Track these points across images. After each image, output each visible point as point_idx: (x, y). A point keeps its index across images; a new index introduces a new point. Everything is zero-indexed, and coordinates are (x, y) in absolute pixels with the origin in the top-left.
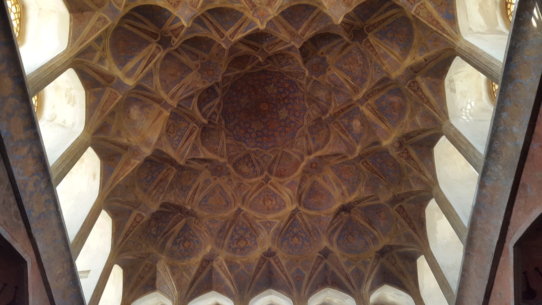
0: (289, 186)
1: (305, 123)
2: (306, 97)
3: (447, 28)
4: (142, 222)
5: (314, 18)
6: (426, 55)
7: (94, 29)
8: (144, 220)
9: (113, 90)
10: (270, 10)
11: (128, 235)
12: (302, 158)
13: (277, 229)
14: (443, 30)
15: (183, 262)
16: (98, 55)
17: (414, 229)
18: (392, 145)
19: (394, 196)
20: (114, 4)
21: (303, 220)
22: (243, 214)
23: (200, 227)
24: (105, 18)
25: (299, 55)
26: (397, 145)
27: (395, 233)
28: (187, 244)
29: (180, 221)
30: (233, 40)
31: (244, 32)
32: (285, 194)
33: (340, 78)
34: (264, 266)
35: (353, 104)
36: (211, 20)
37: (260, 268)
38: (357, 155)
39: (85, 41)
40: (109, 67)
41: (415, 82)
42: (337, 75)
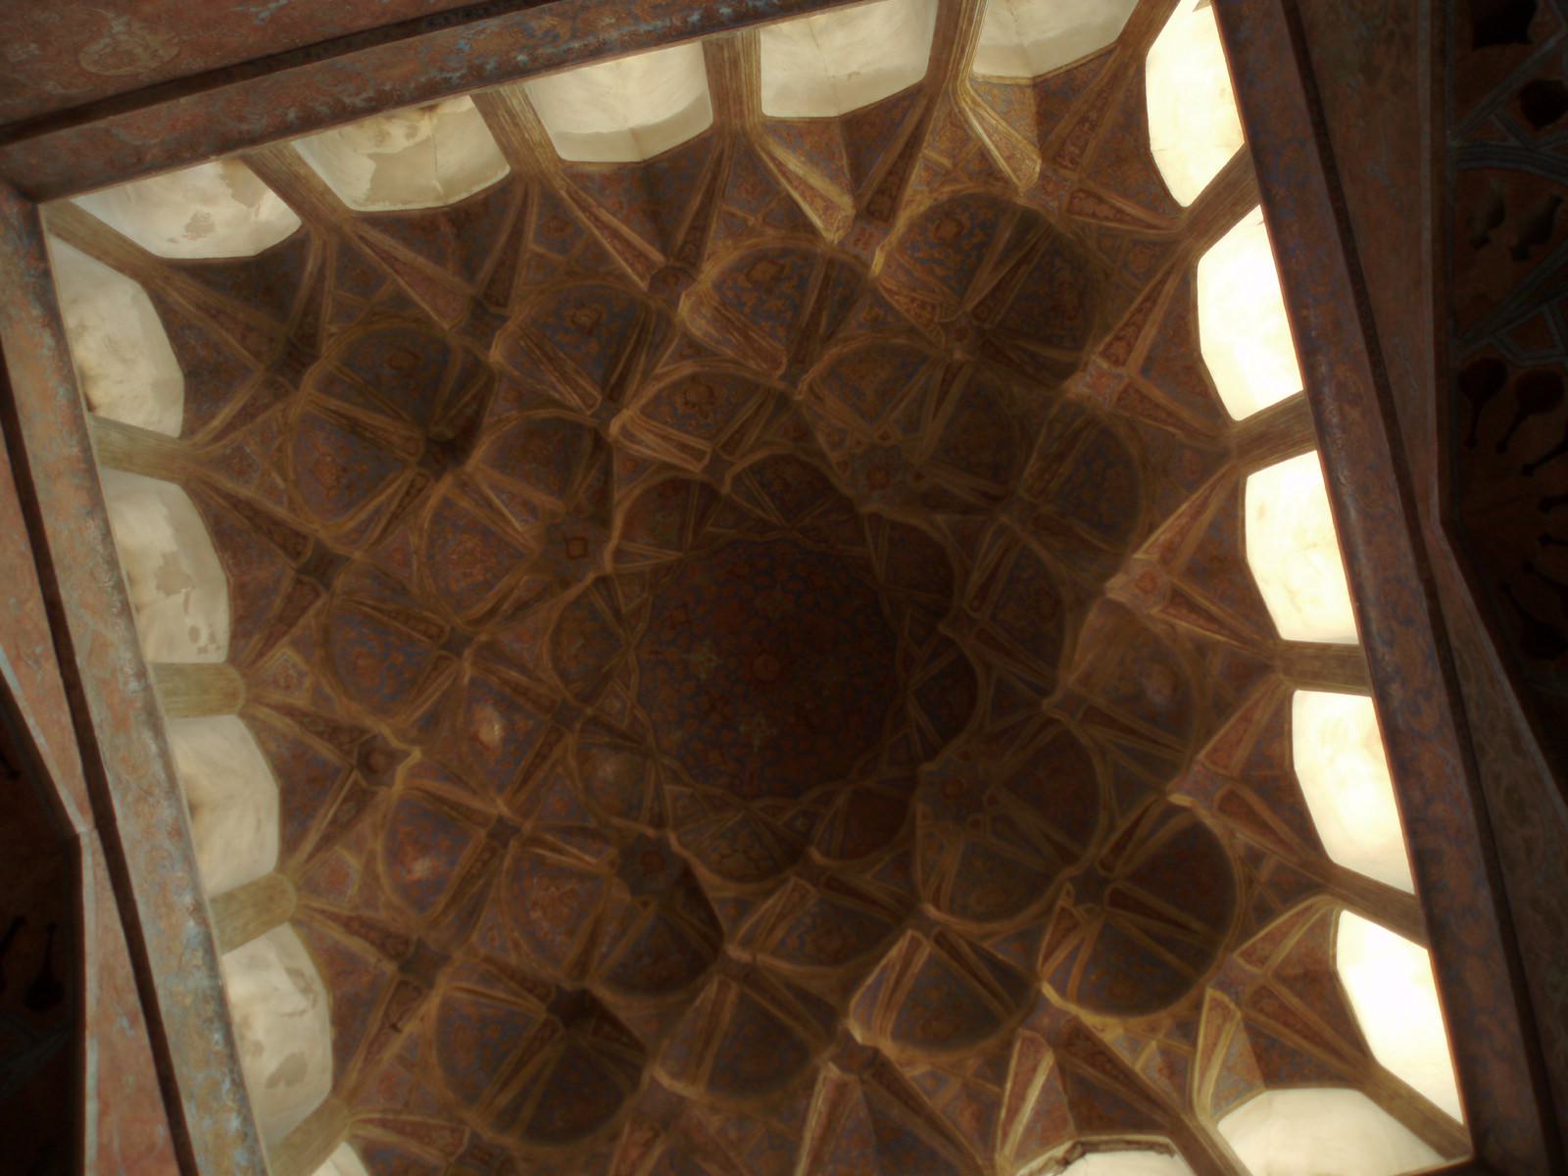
0: (639, 465)
3: (376, 1133)
4: (1108, 339)
6: (396, 1045)
7: (1276, 939)
8: (1101, 347)
9: (1222, 771)
11: (1148, 298)
12: (618, 554)
14: (384, 1124)
15: (953, 191)
16: (1265, 872)
17: (236, 503)
18: (394, 757)
19: (328, 586)
20: (1226, 999)
22: (781, 363)
23: (913, 300)
24: (1250, 963)
25: (710, 895)
26: (378, 760)
27: (280, 449)
28: (949, 230)
29: (981, 303)
30: (909, 933)
32: (648, 438)
33: (575, 851)
34: (680, 238)
35: (518, 791)
36: (976, 984)
37: (693, 228)
38: (467, 653)
39: (1298, 914)
40: (1236, 838)
41: (395, 956)
42: (587, 858)
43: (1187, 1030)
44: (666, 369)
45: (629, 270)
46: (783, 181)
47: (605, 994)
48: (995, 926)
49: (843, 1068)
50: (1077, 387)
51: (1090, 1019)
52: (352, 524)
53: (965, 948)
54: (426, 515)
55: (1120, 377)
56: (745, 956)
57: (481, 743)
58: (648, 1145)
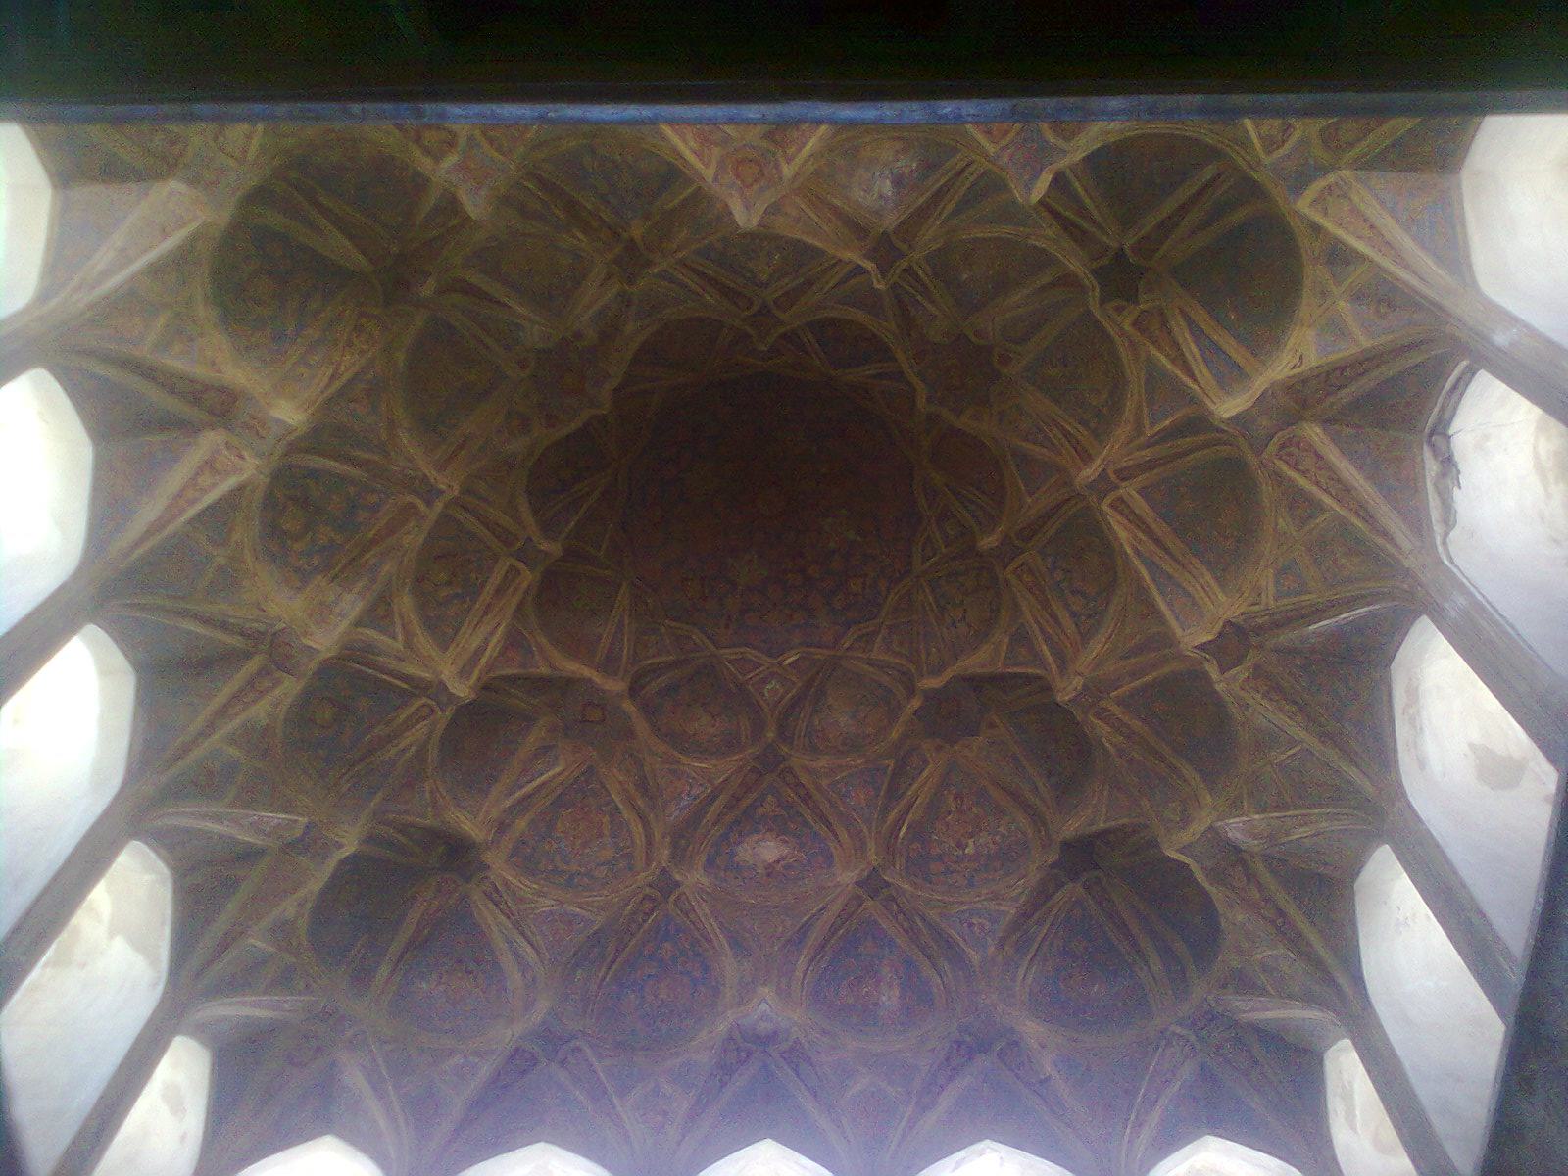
0: (514, 641)
1: (727, 653)
2: (821, 654)
3: (1146, 1134)
5: (1163, 759)
10: (1240, 673)
12: (608, 666)
13: (369, 648)
20: (1318, 185)
21: (407, 725)
22: (413, 506)
25: (999, 669)
26: (764, 1027)
30: (1105, 507)
31: (1138, 553)
32: (484, 630)
34: (235, 641)
35: (836, 835)
38: (678, 877)
42: (925, 774)
43: (1339, 256)
44: (400, 637)
45: (269, 698)
46: (171, 529)
47: (1072, 827)
48: (1130, 406)
49: (1238, 662)
50: (475, 204)
51: (1280, 368)
52: (518, 976)
53: (1147, 454)
54: (526, 886)
55: (471, 139)
56: (1078, 682)
57: (778, 862)
58: (1251, 877)
